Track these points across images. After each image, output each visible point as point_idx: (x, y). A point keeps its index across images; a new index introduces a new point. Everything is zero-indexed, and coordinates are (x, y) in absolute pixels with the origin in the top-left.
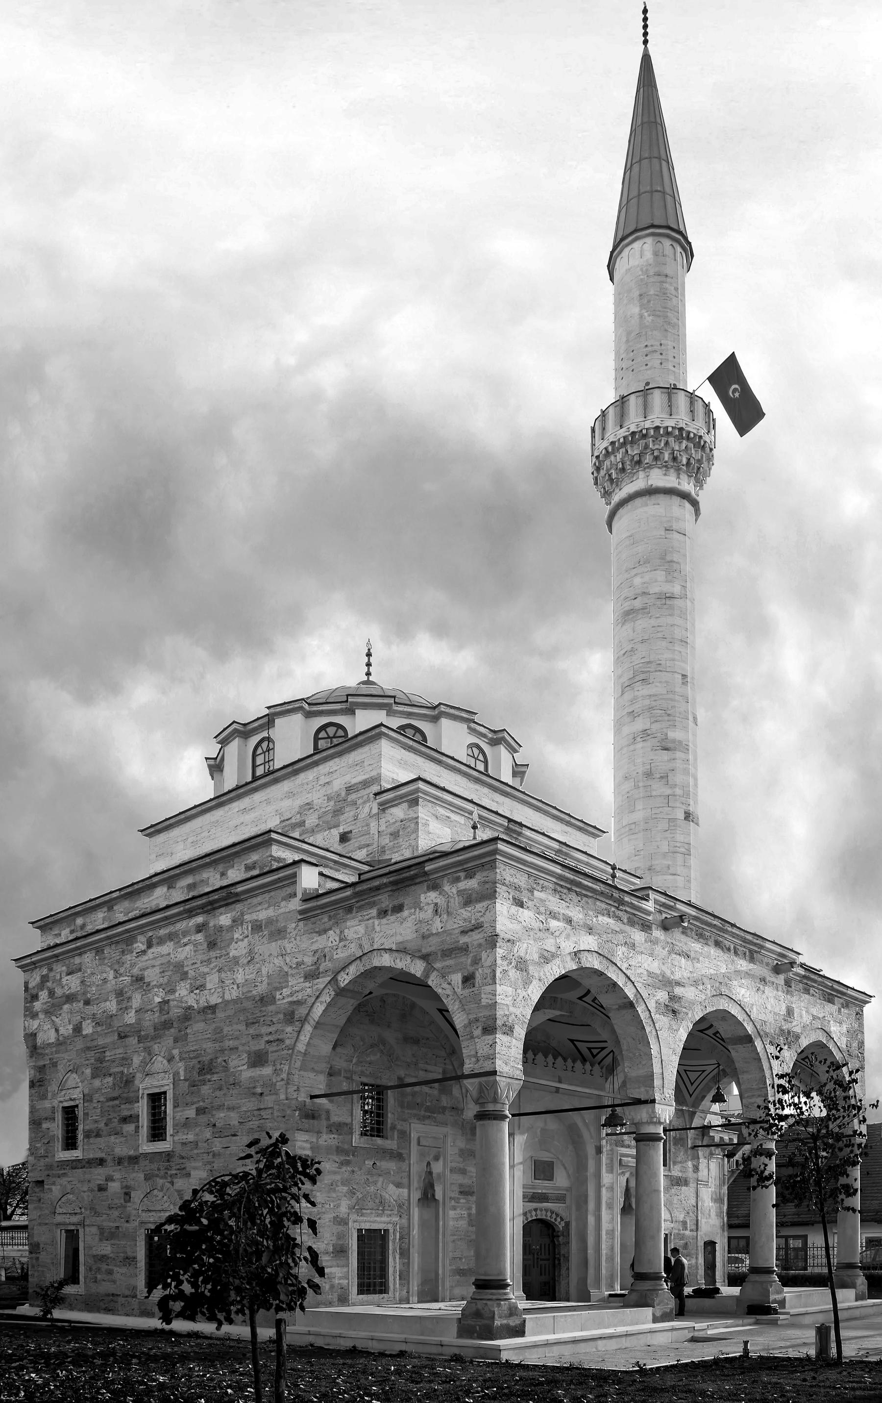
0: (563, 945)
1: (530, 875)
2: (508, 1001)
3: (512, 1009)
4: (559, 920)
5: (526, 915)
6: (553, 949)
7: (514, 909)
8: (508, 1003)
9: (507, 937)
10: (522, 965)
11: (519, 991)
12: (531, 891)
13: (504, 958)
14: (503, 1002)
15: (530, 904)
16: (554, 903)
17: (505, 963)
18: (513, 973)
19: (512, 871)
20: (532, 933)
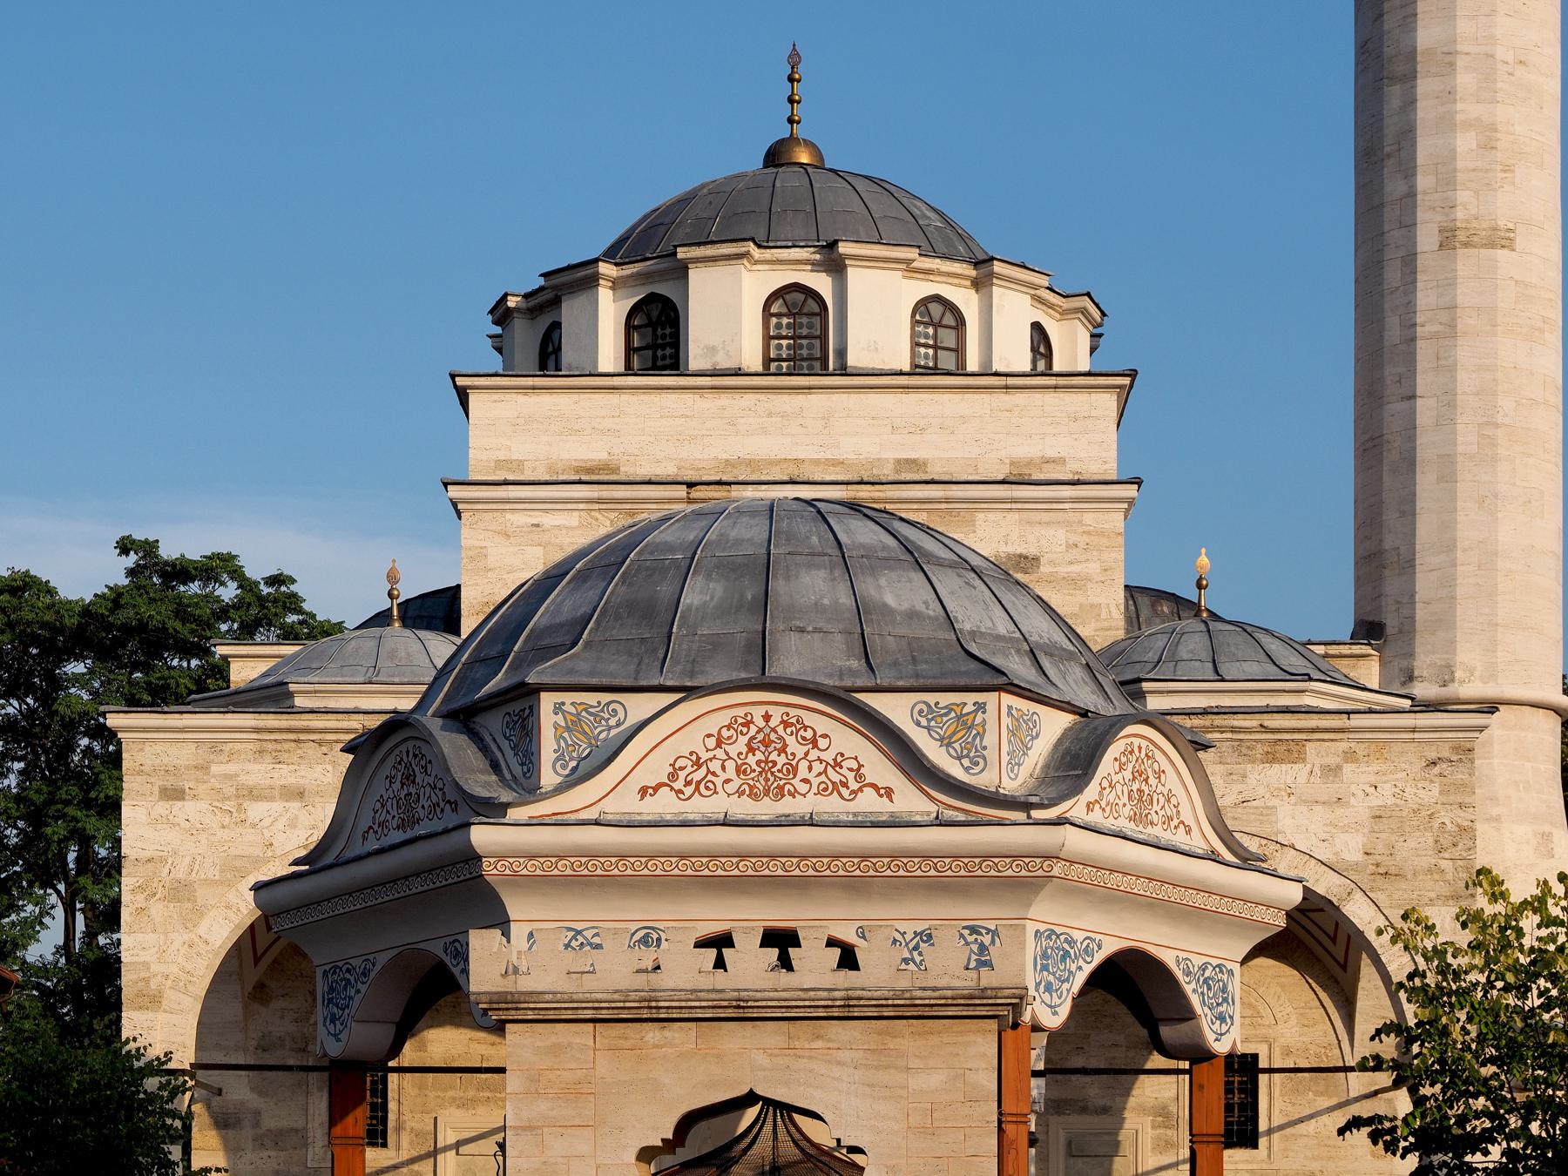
0: (279, 839)
1: (197, 741)
2: (144, 957)
3: (155, 968)
4: (271, 799)
5: (188, 809)
6: (257, 851)
7: (162, 807)
8: (147, 959)
9: (148, 854)
10: (181, 892)
11: (172, 936)
12: (204, 768)
13: (141, 888)
14: (136, 959)
15: (202, 788)
16: (258, 773)
17: (140, 897)
18: (157, 910)
19: (159, 748)
20: (203, 837)
